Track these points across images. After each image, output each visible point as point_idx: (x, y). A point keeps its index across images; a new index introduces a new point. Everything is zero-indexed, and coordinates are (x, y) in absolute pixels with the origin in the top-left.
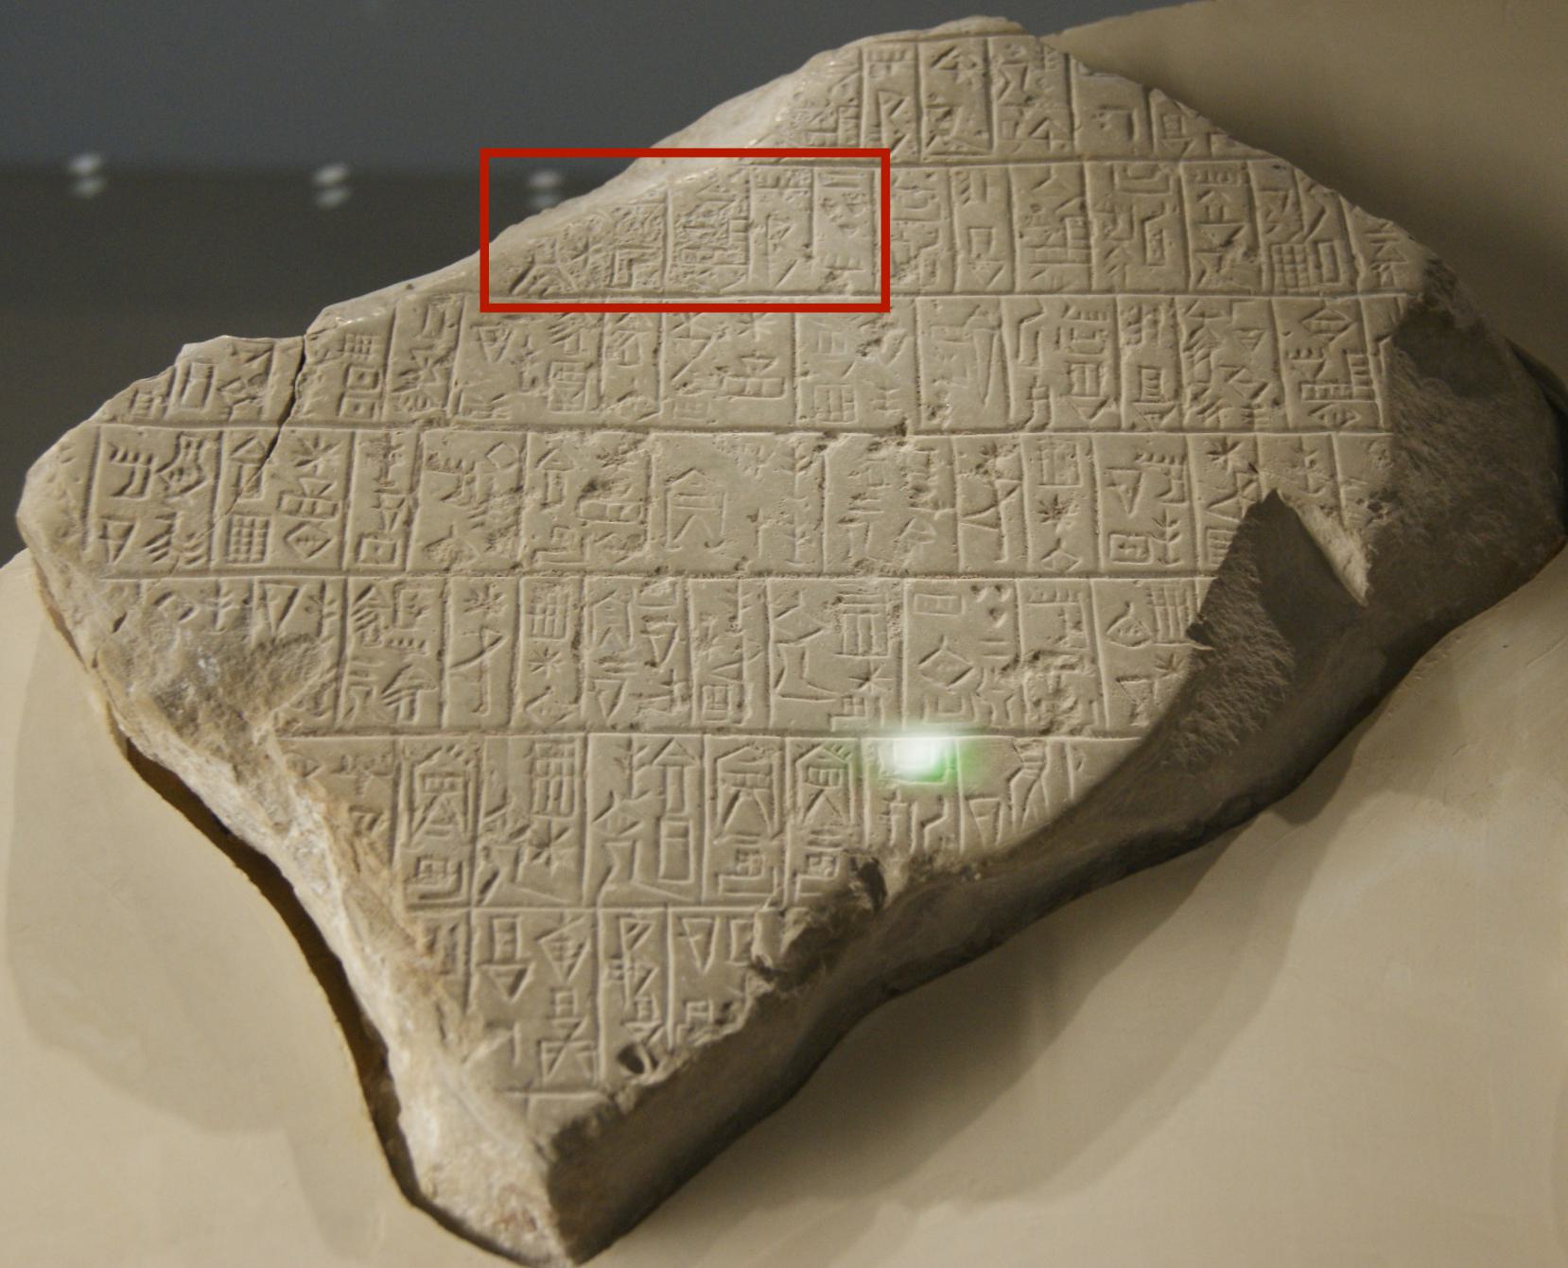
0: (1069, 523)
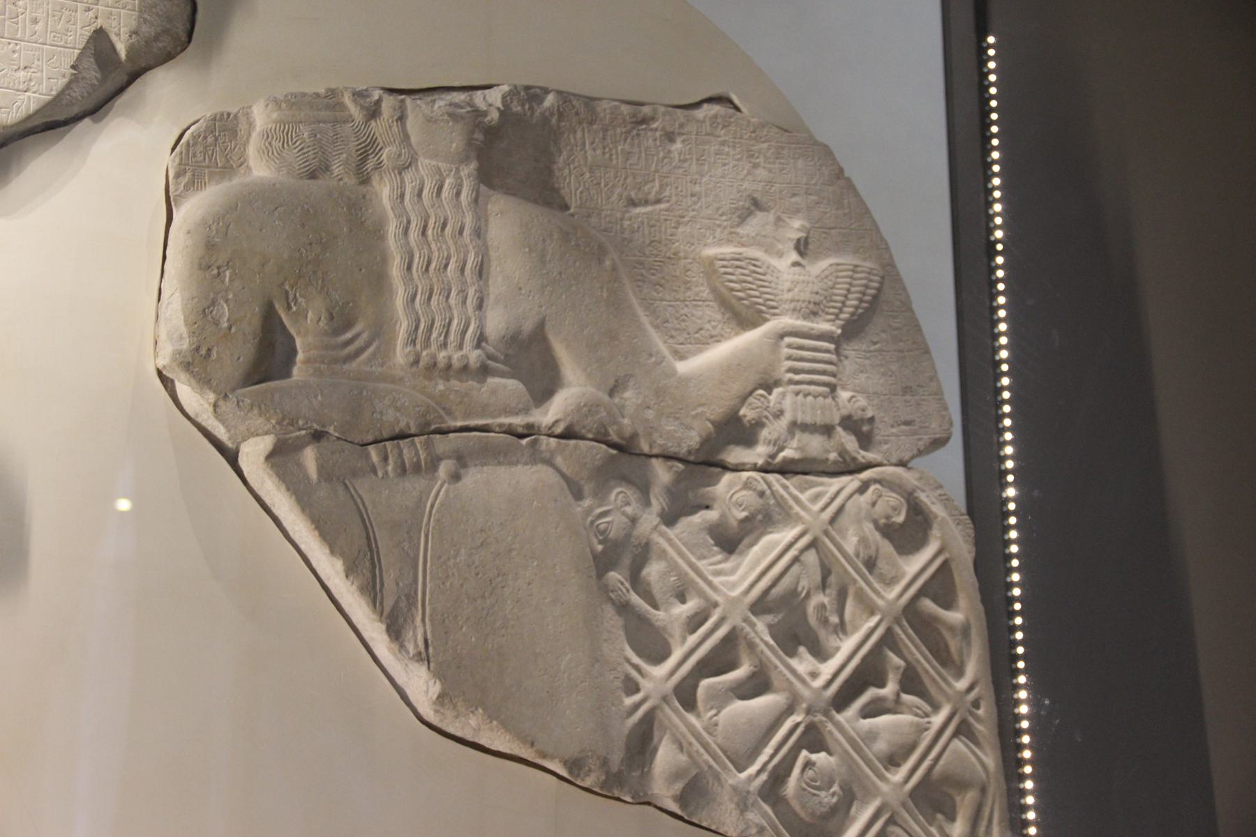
0: (39, 27)
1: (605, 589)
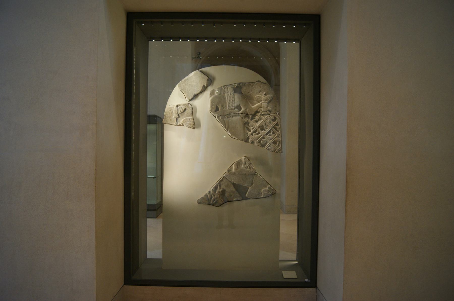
1: (245, 126)
